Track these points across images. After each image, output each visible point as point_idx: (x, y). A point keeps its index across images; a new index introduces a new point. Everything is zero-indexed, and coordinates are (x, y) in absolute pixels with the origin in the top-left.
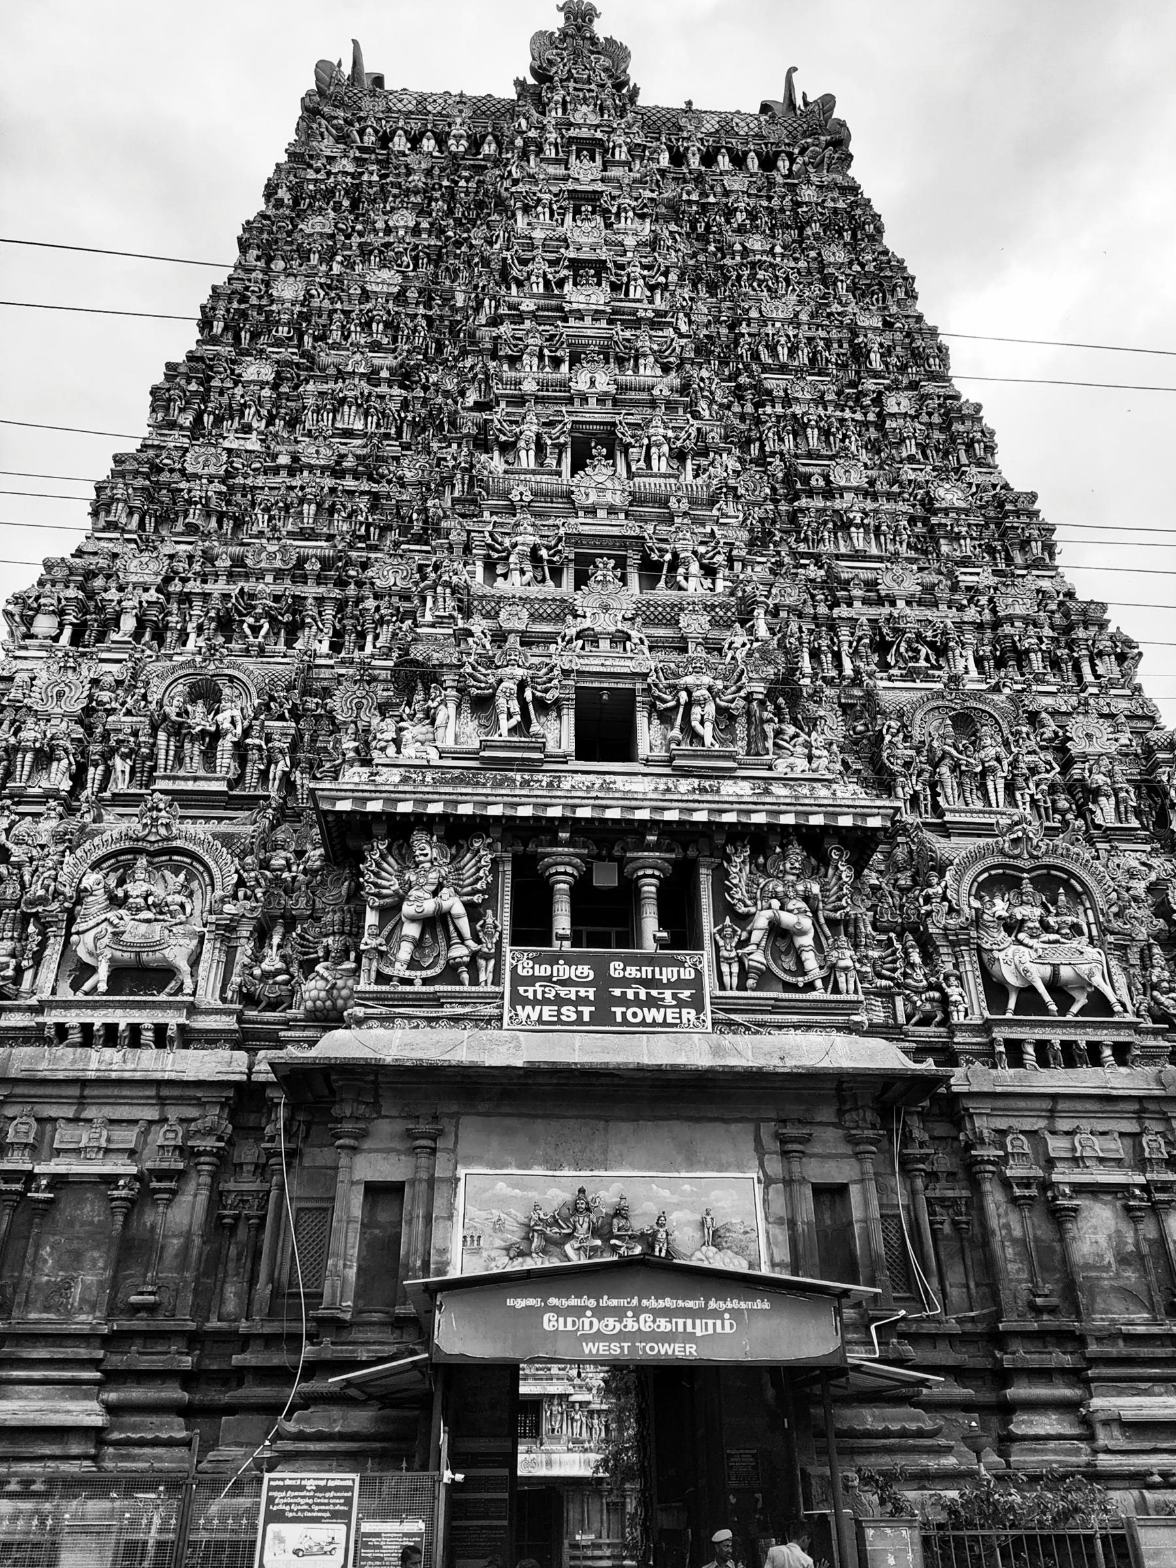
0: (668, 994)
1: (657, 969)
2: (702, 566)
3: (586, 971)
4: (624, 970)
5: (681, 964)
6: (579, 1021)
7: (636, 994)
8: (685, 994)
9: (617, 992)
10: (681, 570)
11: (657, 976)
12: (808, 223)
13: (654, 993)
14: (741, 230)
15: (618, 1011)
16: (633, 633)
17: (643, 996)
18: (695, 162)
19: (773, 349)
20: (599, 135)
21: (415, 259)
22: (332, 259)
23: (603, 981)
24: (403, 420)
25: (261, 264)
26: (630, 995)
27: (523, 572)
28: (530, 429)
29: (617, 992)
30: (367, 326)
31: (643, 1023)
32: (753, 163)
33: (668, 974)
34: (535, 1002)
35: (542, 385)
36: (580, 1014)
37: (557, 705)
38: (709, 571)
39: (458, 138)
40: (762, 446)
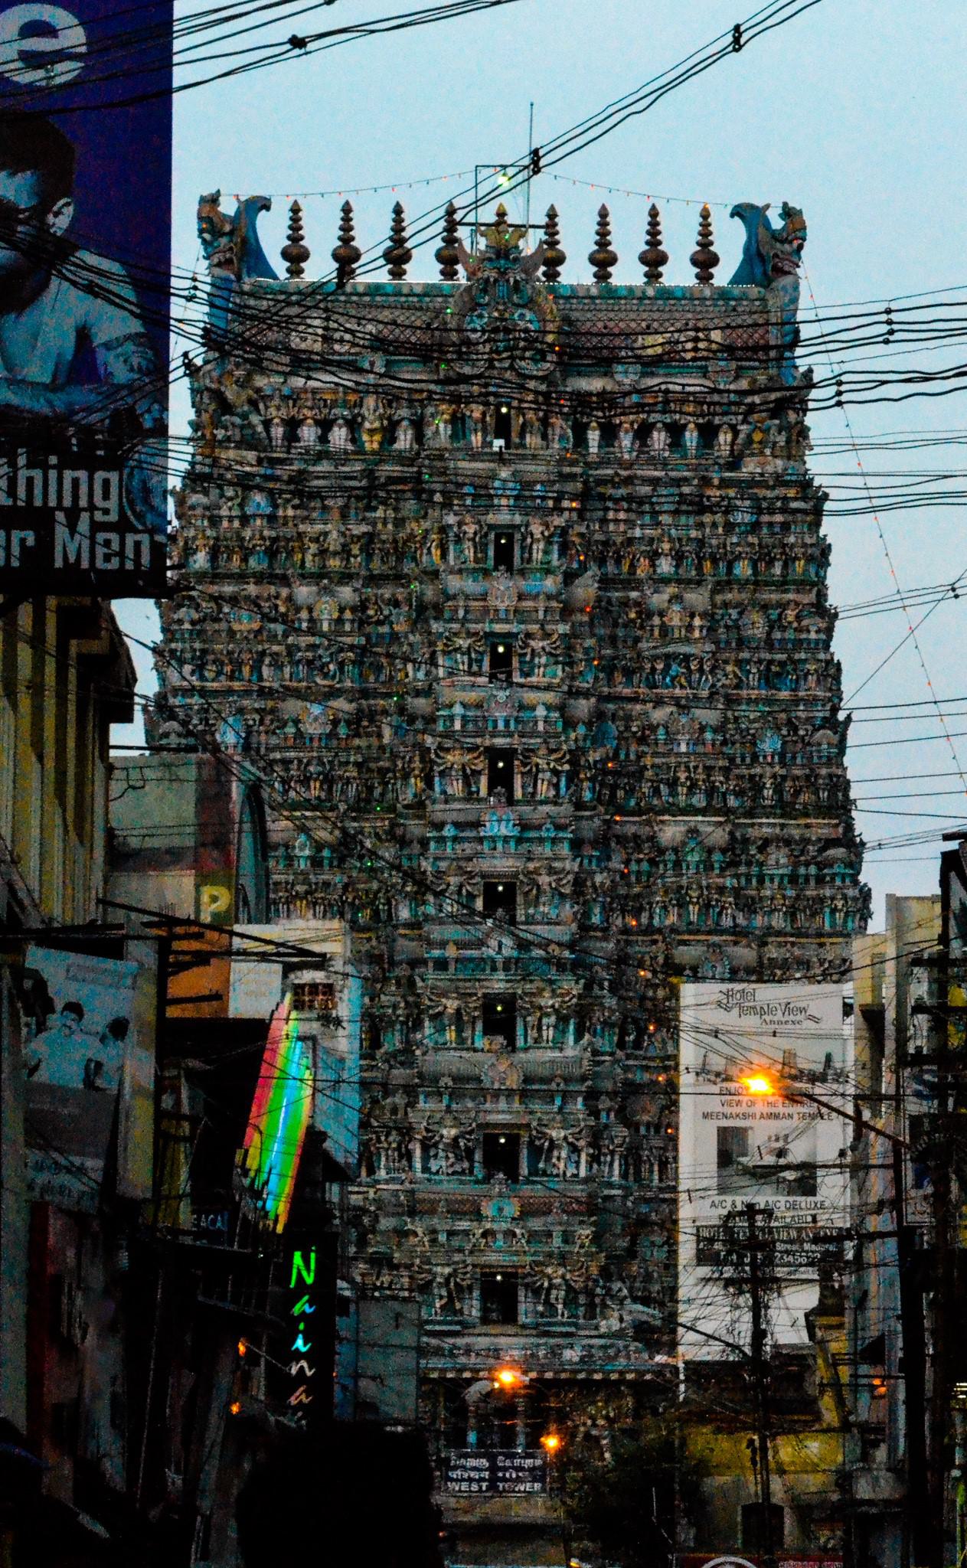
2: (569, 1144)
3: (484, 1463)
6: (480, 1490)
9: (500, 1474)
10: (556, 1153)
12: (738, 557)
14: (665, 581)
16: (518, 1231)
18: (626, 440)
19: (673, 784)
20: (518, 519)
21: (341, 665)
22: (262, 662)
23: (493, 1469)
24: (343, 902)
25: (195, 681)
27: (447, 1158)
28: (451, 1005)
29: (500, 1474)
30: (305, 781)
32: (691, 437)
34: (457, 1480)
35: (460, 945)
37: (470, 1288)
38: (575, 1149)
39: (372, 432)
40: (651, 918)
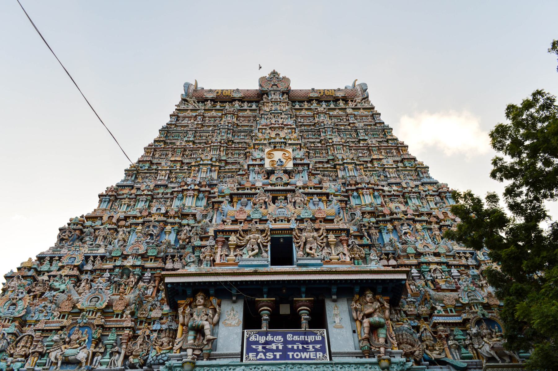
0: (311, 346)
1: (306, 337)
4: (293, 337)
5: (316, 334)
7: (298, 347)
8: (318, 346)
9: (290, 346)
11: (306, 339)
13: (305, 346)
15: (290, 354)
17: (300, 348)
26: (295, 347)
29: (290, 346)
31: (301, 359)
33: (310, 338)
36: (275, 356)
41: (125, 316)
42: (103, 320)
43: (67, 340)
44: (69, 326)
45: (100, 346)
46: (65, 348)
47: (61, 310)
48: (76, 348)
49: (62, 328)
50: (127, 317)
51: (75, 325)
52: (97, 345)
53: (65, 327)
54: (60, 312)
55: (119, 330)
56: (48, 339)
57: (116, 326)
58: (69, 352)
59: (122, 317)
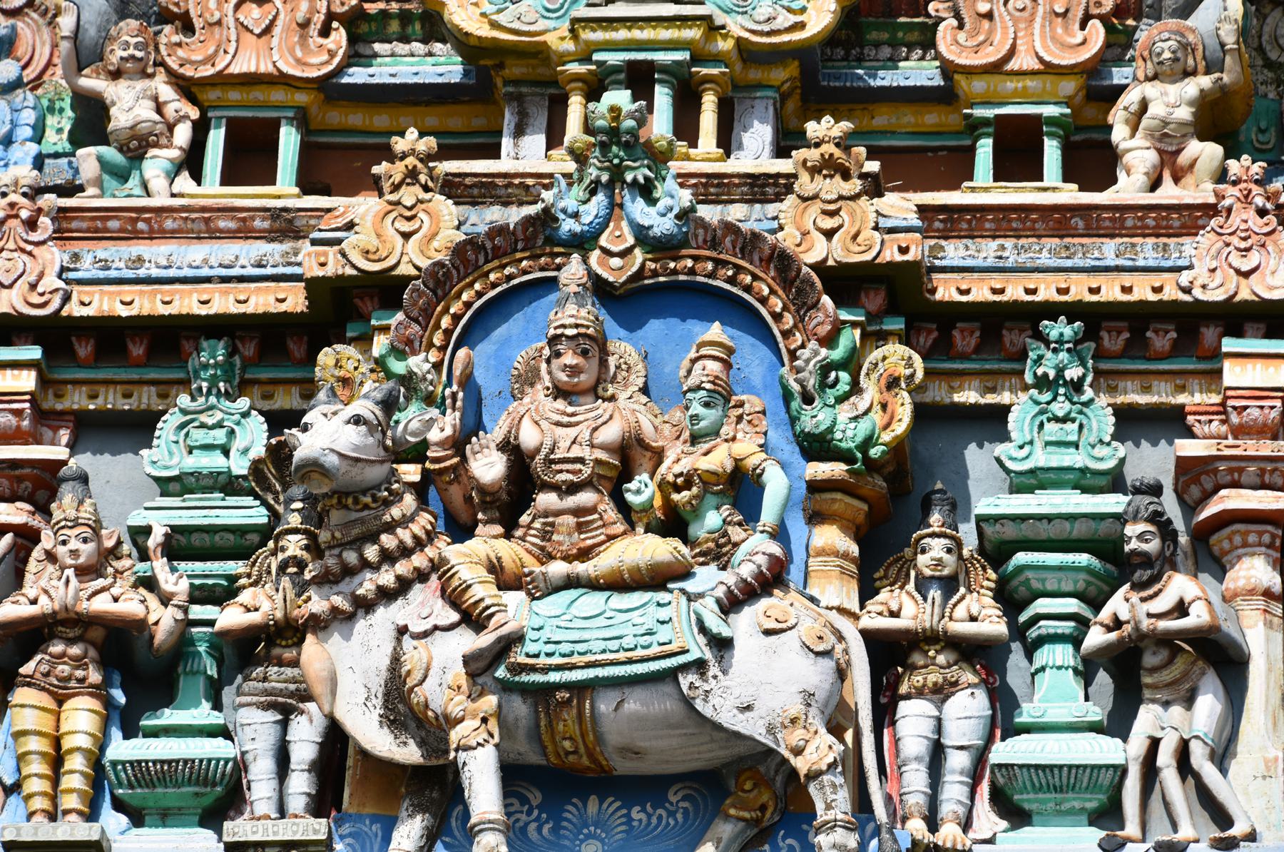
41: (1138, 157)
42: (900, 206)
43: (488, 467)
44: (441, 281)
45: (933, 554)
46: (506, 579)
47: (194, 56)
48: (656, 579)
49: (345, 306)
50: (1170, 164)
51: (499, 277)
52: (878, 561)
53: (386, 289)
54: (187, 88)
55: (1137, 347)
56: (167, 452)
57: (1079, 290)
58: (569, 629)
59: (1093, 160)
